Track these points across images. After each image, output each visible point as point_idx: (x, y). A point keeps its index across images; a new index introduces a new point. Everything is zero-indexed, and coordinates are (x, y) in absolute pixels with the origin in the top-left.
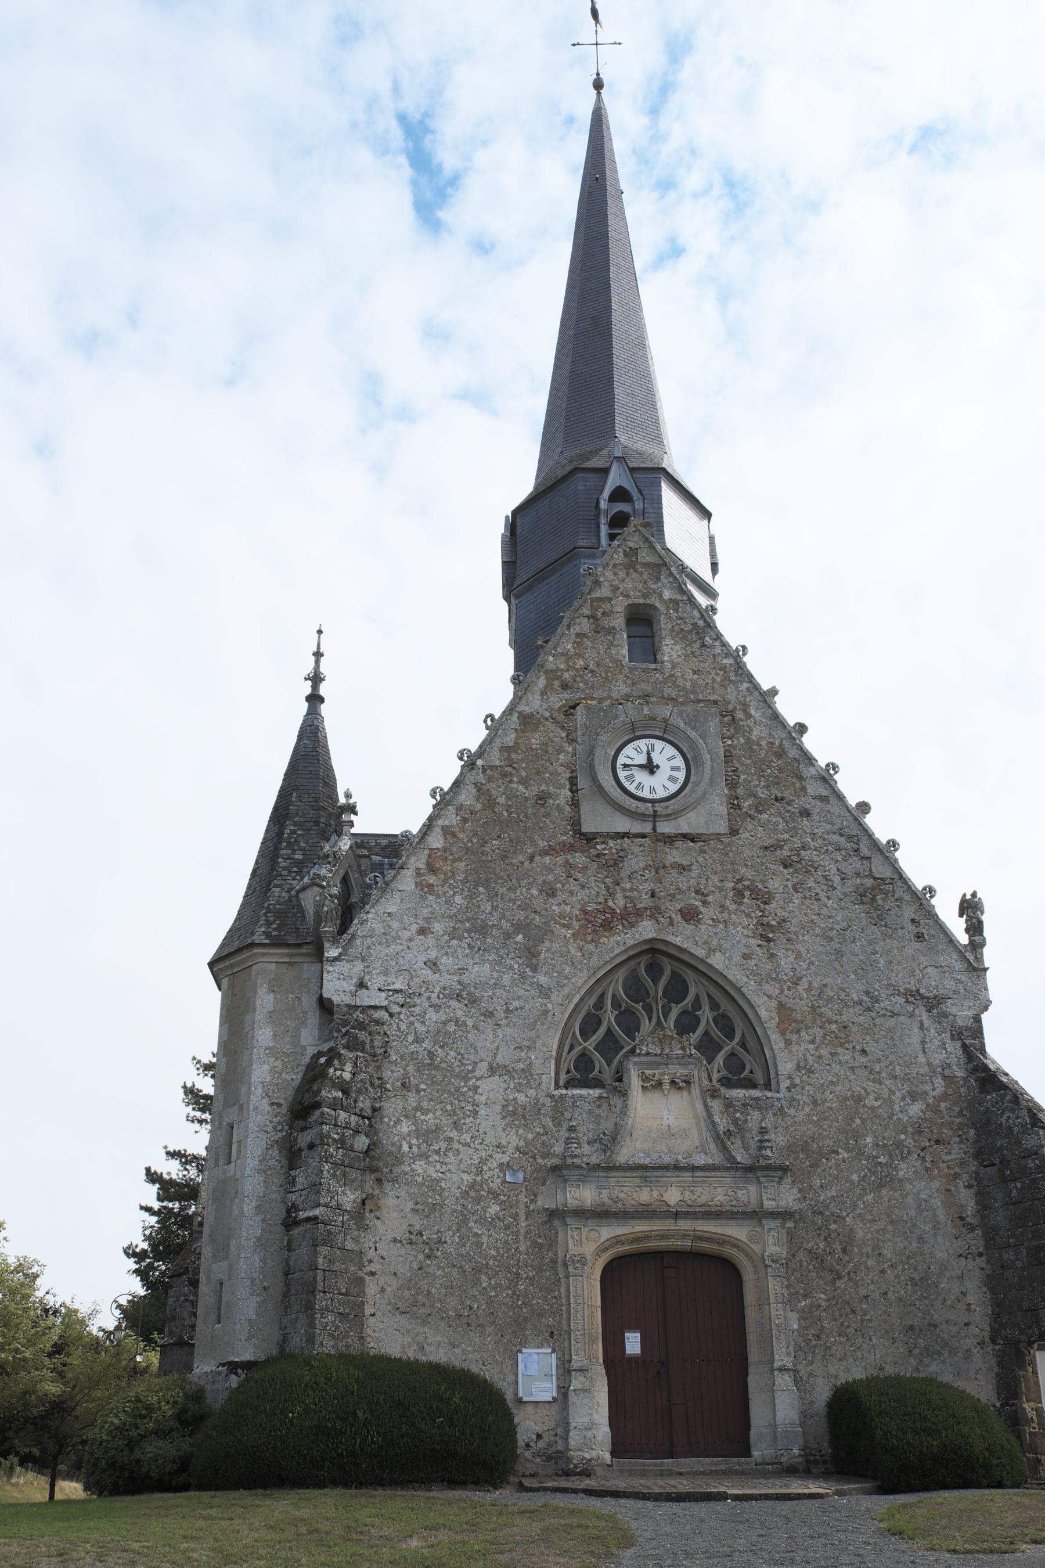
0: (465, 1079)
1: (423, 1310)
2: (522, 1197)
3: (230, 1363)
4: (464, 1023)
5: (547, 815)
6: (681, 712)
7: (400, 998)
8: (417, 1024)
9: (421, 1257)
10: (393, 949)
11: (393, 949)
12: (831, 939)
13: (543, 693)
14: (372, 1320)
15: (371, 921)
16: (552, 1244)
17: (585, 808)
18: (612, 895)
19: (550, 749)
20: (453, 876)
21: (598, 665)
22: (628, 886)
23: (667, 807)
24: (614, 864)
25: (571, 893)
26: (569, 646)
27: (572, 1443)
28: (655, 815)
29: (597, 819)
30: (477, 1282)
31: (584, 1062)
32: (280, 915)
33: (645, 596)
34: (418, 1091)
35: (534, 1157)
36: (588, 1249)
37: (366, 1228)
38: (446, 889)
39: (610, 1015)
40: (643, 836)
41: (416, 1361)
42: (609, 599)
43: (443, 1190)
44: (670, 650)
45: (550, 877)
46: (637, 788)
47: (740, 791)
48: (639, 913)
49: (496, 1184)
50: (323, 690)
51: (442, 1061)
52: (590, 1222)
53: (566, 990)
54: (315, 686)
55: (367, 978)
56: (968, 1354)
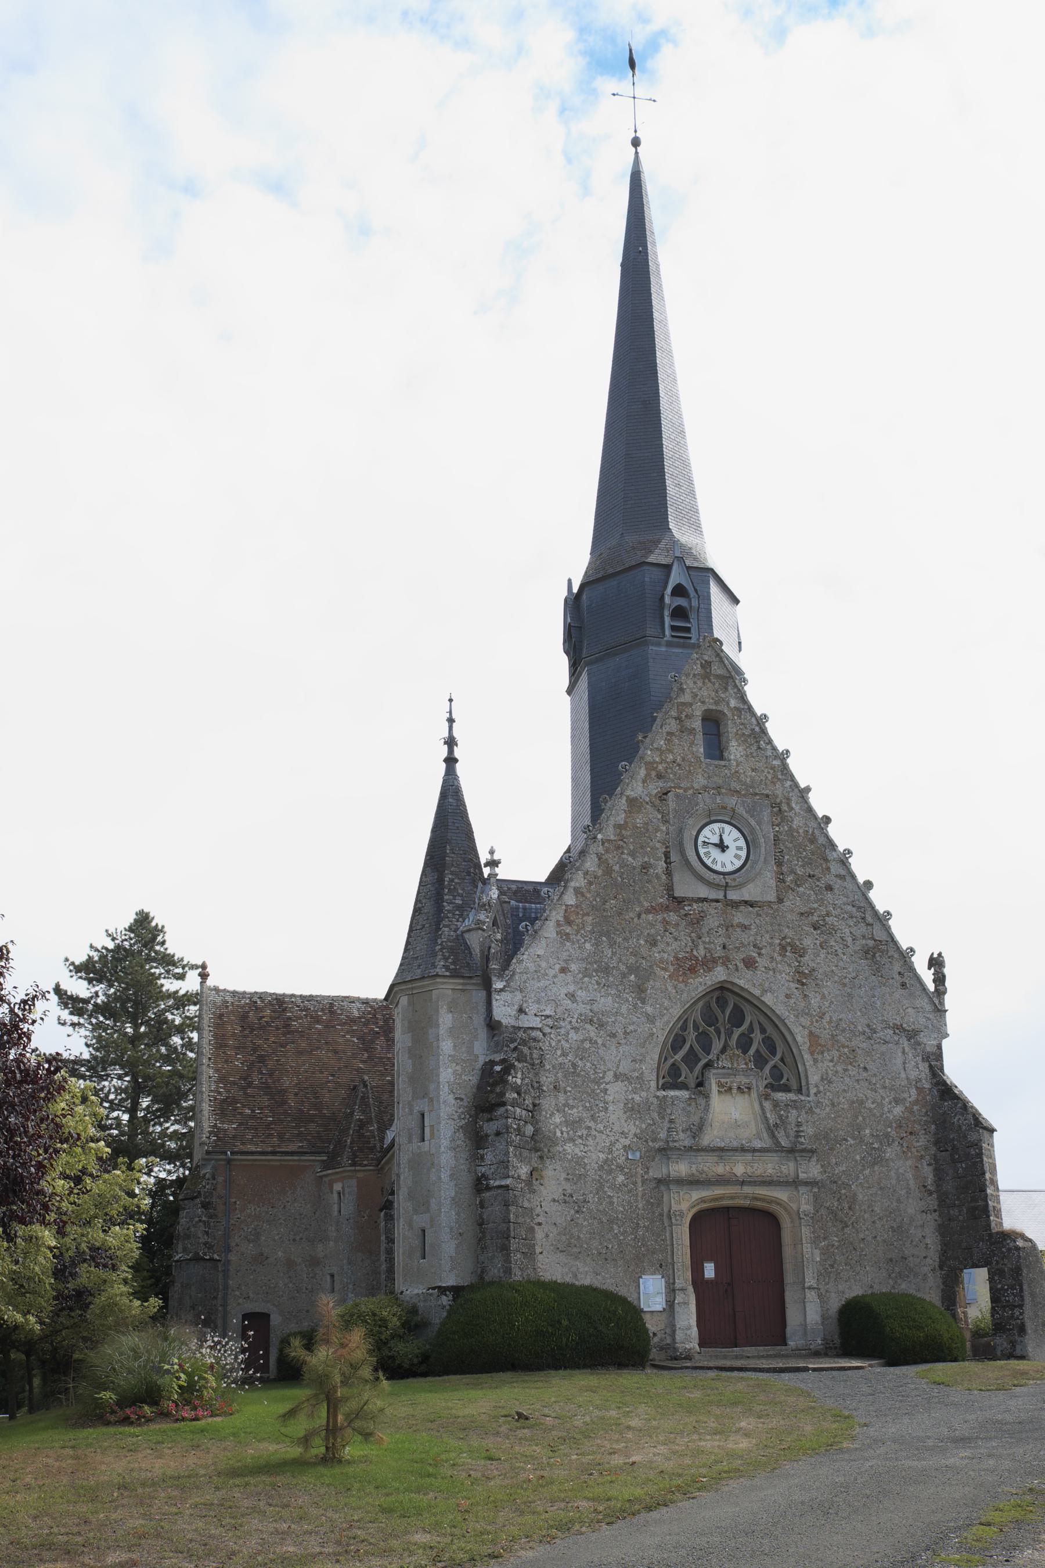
0: (598, 1083)
1: (575, 1250)
2: (639, 1169)
3: (439, 1287)
4: (596, 1042)
5: (649, 881)
6: (744, 802)
7: (550, 1022)
8: (563, 1042)
9: (572, 1212)
10: (541, 984)
11: (541, 984)
12: (845, 985)
13: (644, 782)
14: (540, 1256)
15: (527, 959)
16: (660, 1203)
17: (676, 878)
18: (696, 946)
19: (650, 828)
20: (583, 928)
21: (683, 760)
22: (707, 940)
23: (734, 880)
24: (696, 922)
25: (668, 944)
26: (662, 742)
27: (677, 1338)
28: (727, 885)
29: (686, 887)
30: (611, 1229)
31: (674, 1071)
32: (452, 951)
33: (716, 703)
34: (565, 1092)
35: (646, 1141)
36: (684, 1206)
37: (534, 1192)
38: (579, 937)
39: (691, 1036)
40: (717, 901)
41: (573, 1285)
42: (691, 705)
43: (586, 1164)
44: (735, 750)
45: (653, 931)
46: (713, 862)
47: (785, 869)
48: (714, 961)
49: (621, 1161)
50: (457, 753)
51: (582, 1070)
52: (685, 1188)
53: (665, 1019)
54: (451, 751)
55: (525, 1005)
56: (925, 1277)
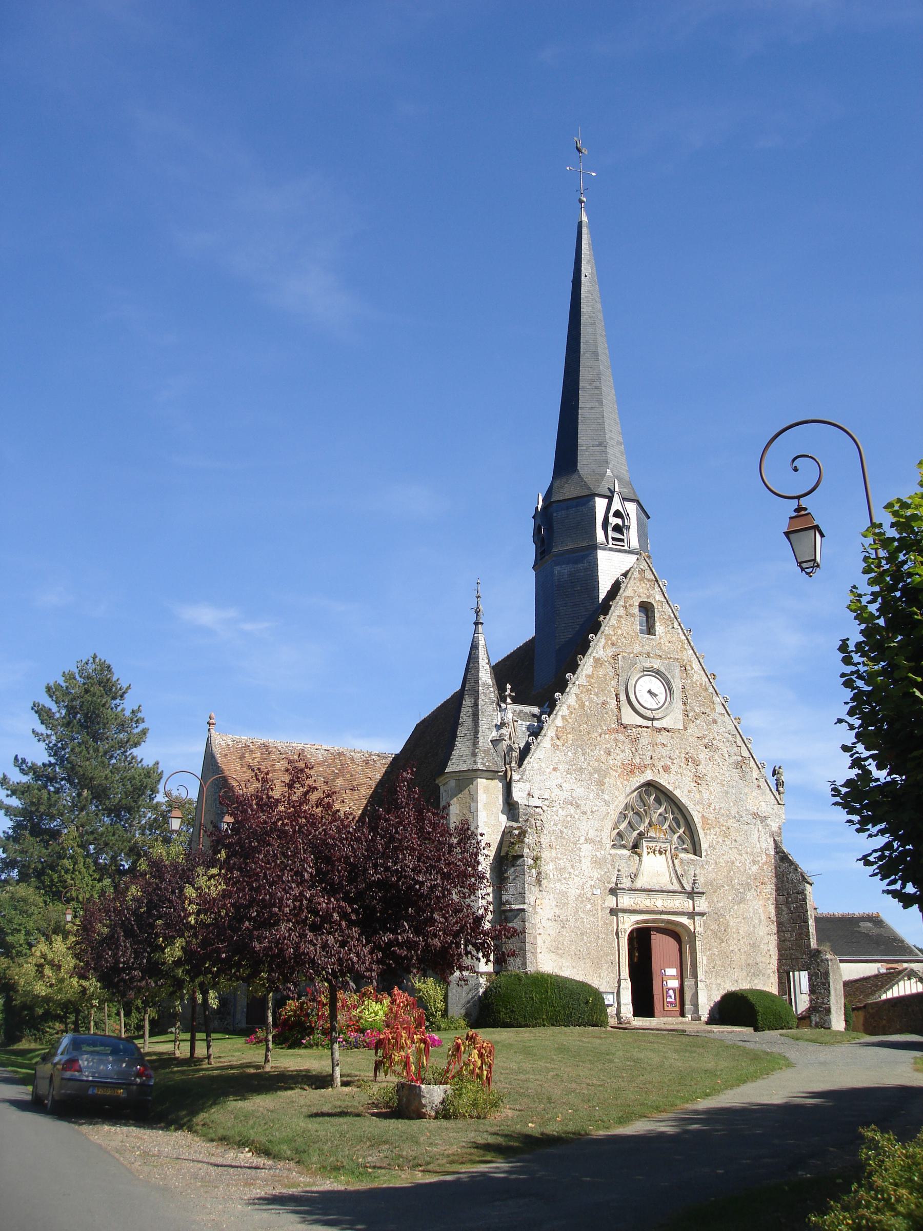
7: (546, 802)
12: (723, 785)
13: (604, 648)
29: (629, 717)
30: (583, 939)
40: (647, 727)
45: (609, 746)
47: (688, 708)
56: (769, 976)
